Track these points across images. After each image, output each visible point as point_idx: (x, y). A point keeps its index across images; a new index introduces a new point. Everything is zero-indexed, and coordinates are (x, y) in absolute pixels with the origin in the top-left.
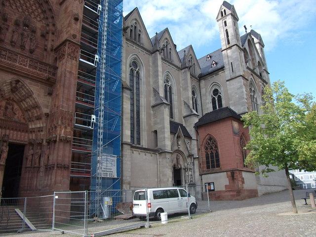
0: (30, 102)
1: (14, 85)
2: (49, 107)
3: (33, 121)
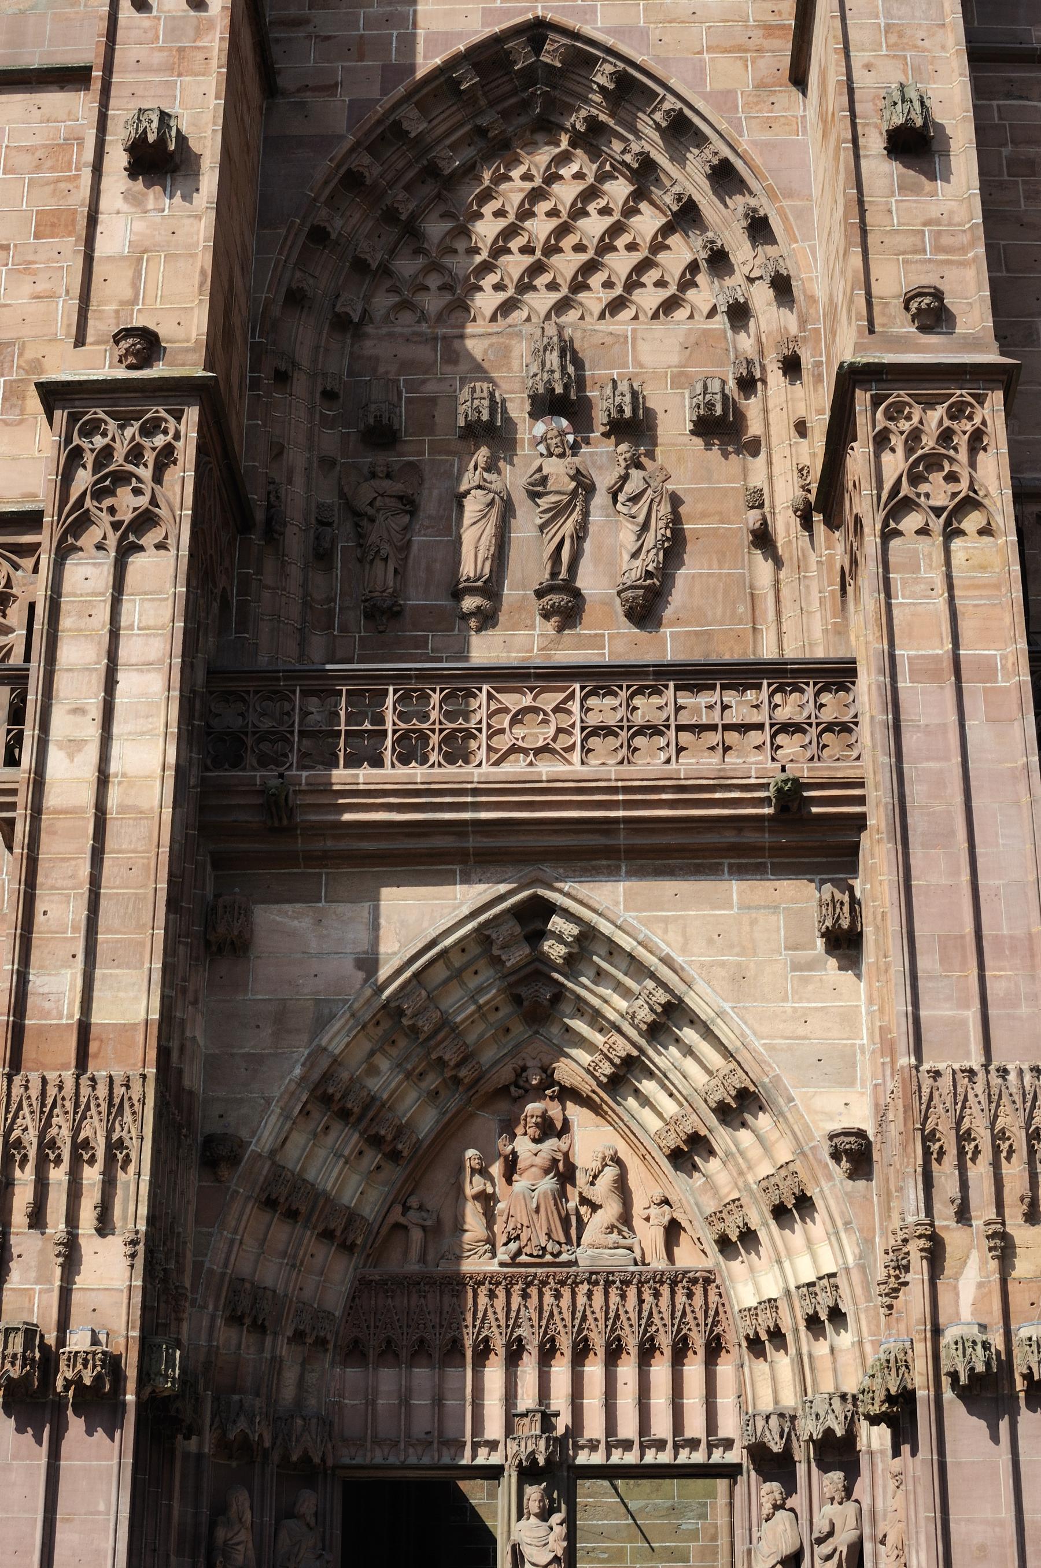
0: (689, 1073)
1: (517, 956)
2: (865, 1067)
3: (749, 1237)
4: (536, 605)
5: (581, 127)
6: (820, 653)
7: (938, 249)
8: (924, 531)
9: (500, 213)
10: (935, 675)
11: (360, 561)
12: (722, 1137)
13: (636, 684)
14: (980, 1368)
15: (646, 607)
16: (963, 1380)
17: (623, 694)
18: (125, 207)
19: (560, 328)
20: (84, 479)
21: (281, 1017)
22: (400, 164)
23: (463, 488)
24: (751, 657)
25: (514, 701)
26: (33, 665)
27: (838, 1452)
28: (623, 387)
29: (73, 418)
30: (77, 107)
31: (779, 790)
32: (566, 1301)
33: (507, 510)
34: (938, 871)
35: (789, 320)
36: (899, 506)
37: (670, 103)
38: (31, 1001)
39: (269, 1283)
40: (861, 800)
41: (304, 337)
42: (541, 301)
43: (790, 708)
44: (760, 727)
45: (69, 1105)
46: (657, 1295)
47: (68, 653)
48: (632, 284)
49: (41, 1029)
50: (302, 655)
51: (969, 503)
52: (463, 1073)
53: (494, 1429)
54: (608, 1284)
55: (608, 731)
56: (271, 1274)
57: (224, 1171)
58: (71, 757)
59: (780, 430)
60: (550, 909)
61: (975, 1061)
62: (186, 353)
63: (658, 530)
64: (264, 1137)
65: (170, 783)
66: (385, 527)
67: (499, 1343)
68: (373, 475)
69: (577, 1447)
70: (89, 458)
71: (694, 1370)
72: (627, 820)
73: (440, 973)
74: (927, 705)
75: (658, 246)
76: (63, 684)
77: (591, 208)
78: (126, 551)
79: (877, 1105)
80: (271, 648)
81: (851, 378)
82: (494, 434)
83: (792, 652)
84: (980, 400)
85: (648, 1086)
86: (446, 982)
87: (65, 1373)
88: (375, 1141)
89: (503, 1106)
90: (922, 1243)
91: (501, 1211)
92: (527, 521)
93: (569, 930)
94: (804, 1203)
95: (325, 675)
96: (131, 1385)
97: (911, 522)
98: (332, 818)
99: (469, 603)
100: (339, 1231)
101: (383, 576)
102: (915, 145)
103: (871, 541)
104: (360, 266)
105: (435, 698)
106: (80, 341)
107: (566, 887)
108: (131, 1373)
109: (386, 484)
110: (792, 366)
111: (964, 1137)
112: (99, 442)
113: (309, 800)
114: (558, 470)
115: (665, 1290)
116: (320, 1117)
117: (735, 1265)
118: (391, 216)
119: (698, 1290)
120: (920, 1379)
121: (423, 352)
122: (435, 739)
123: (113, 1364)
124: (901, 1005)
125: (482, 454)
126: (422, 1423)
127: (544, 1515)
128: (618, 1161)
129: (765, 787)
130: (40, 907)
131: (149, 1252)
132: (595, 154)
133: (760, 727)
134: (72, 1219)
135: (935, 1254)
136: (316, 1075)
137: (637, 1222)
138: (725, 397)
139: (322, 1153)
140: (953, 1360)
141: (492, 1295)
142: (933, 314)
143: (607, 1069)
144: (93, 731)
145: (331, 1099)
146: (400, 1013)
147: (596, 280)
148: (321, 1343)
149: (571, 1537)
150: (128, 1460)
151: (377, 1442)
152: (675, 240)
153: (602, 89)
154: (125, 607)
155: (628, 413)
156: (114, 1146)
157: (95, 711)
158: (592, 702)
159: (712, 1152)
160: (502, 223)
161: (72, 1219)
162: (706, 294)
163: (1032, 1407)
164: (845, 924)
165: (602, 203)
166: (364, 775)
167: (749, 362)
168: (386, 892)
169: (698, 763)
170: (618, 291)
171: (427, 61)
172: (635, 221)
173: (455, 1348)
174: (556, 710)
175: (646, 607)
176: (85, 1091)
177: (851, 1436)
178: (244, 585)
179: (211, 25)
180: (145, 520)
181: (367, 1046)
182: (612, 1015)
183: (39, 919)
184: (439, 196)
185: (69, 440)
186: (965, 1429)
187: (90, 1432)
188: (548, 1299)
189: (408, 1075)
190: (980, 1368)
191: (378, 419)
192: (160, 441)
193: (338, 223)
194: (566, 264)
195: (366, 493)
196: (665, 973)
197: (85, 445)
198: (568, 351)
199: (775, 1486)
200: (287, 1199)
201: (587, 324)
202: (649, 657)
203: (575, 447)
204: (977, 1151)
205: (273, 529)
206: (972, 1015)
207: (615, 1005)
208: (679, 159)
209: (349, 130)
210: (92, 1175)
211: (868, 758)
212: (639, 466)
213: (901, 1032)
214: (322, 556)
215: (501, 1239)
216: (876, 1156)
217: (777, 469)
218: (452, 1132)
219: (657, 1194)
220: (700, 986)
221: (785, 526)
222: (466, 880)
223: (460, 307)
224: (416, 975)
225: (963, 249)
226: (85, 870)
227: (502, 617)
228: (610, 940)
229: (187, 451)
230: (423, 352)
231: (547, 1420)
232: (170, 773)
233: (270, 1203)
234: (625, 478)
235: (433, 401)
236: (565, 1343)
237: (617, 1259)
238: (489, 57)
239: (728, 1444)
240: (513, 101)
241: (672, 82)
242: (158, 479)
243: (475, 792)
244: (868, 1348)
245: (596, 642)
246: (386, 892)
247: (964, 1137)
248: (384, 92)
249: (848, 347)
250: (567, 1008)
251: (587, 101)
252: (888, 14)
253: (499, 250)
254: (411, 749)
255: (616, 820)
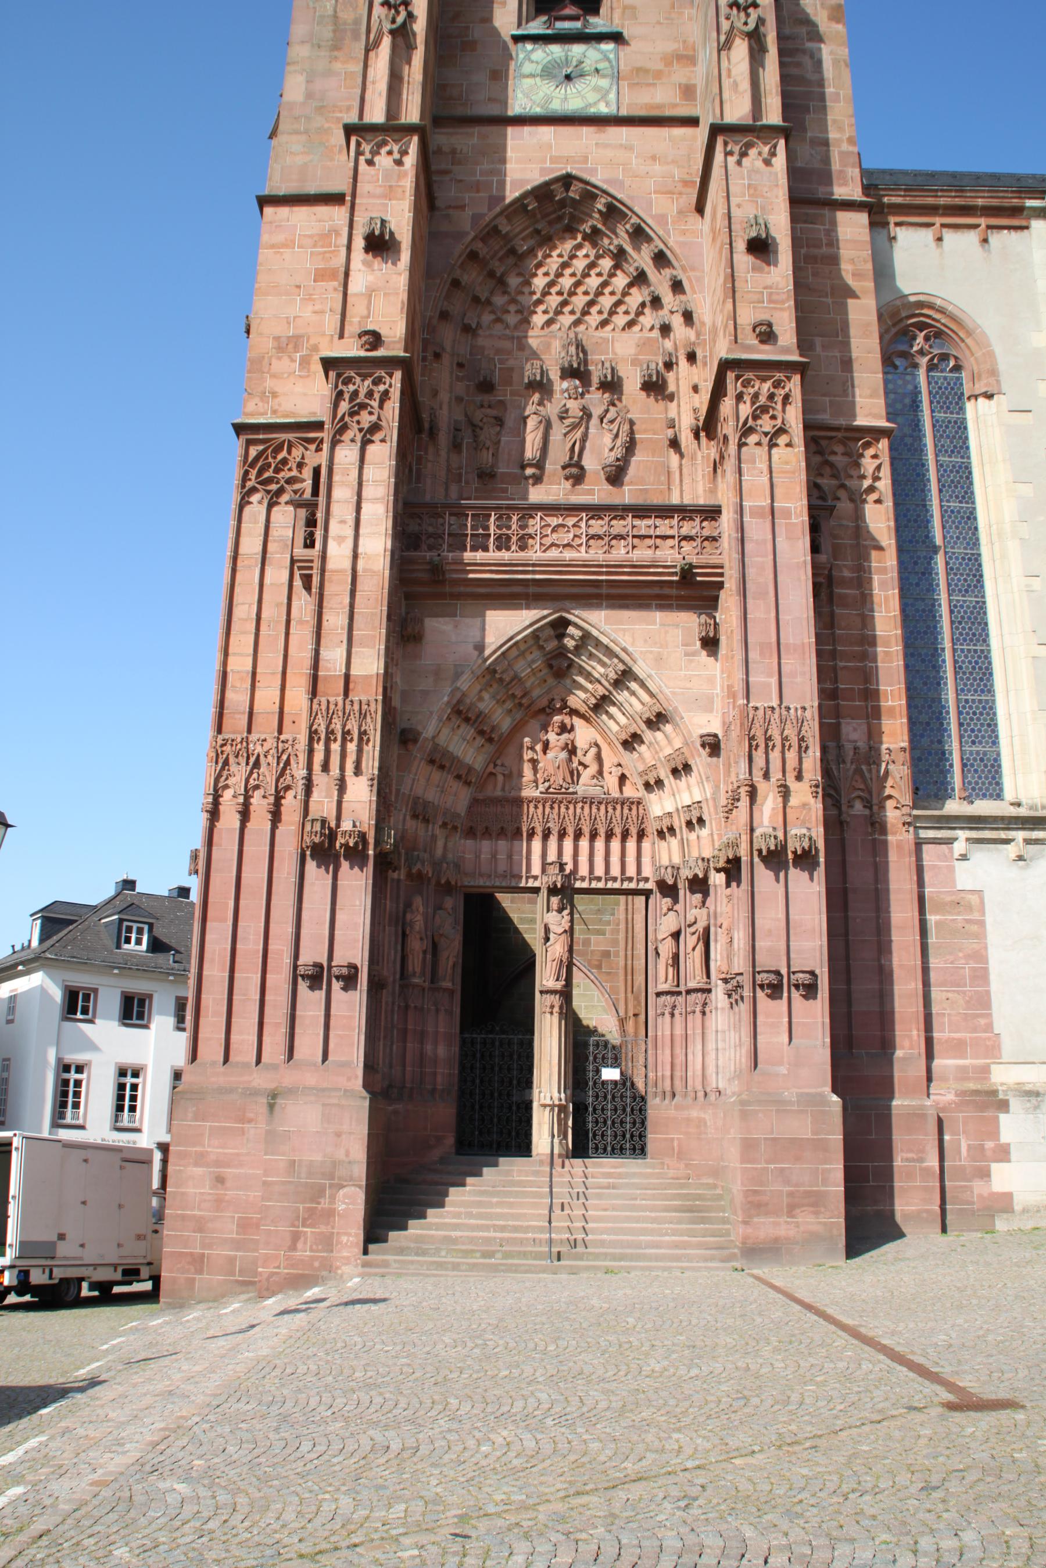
0: (633, 704)
1: (551, 645)
2: (718, 704)
4: (562, 473)
5: (588, 231)
6: (701, 502)
7: (770, 301)
8: (758, 444)
9: (546, 274)
10: (762, 516)
11: (475, 449)
12: (648, 735)
13: (613, 514)
14: (773, 848)
15: (616, 476)
16: (764, 853)
17: (607, 519)
18: (363, 268)
19: (576, 334)
20: (344, 406)
21: (437, 673)
22: (497, 248)
23: (527, 413)
24: (667, 503)
25: (554, 521)
26: (320, 499)
27: (700, 885)
28: (607, 365)
29: (339, 376)
30: (338, 215)
31: (682, 569)
32: (571, 811)
33: (548, 426)
34: (760, 611)
35: (691, 334)
36: (747, 431)
37: (635, 220)
38: (321, 663)
39: (430, 799)
40: (721, 575)
41: (448, 335)
42: (566, 320)
43: (687, 528)
44: (673, 537)
45: (340, 714)
46: (614, 809)
47: (338, 493)
48: (612, 313)
49: (326, 677)
50: (447, 495)
51: (781, 431)
52: (524, 701)
53: (536, 870)
54: (592, 803)
55: (599, 537)
56: (431, 795)
57: (410, 746)
58: (339, 544)
59: (685, 389)
60: (567, 623)
61: (775, 703)
62: (395, 345)
63: (623, 437)
64: (429, 731)
65: (388, 559)
66: (488, 433)
67: (539, 830)
68: (482, 406)
69: (575, 879)
70: (347, 396)
71: (631, 845)
72: (607, 581)
73: (515, 652)
74: (757, 530)
75: (625, 294)
76: (335, 508)
77: (593, 273)
78: (366, 443)
79: (724, 723)
80: (432, 492)
81: (725, 366)
82: (542, 387)
83: (686, 501)
84: (789, 379)
85: (612, 710)
86: (517, 657)
87: (340, 840)
88: (481, 733)
89: (542, 717)
90: (747, 788)
91: (541, 767)
92: (558, 431)
93: (577, 633)
94: (687, 768)
95: (461, 506)
96: (371, 846)
97: (752, 439)
98: (463, 576)
99: (529, 471)
100: (464, 776)
101: (486, 457)
102: (761, 247)
103: (732, 448)
104: (476, 300)
105: (515, 518)
106: (341, 336)
107: (576, 612)
108: (371, 841)
109: (489, 411)
110: (691, 357)
111: (768, 739)
112: (352, 388)
113: (453, 567)
114: (574, 406)
115: (619, 807)
116: (456, 721)
117: (652, 796)
118: (491, 274)
119: (634, 807)
120: (743, 852)
121: (506, 344)
122: (514, 539)
123: (363, 836)
124: (740, 675)
125: (536, 397)
126: (502, 867)
127: (560, 911)
128: (597, 745)
129: (675, 567)
130: (325, 617)
131: (379, 784)
132: (594, 245)
133: (673, 537)
134: (342, 768)
135: (753, 794)
136: (455, 701)
137: (606, 774)
138: (658, 372)
139: (456, 738)
140: (760, 843)
141: (536, 807)
142: (767, 335)
143: (593, 701)
144: (350, 532)
145: (461, 713)
146: (495, 671)
147: (594, 310)
148: (455, 828)
149: (572, 921)
150: (370, 881)
151: (481, 875)
152: (634, 291)
153: (600, 211)
154: (365, 471)
155: (609, 378)
156: (362, 734)
157: (351, 523)
158: (592, 522)
159: (642, 742)
160: (547, 279)
161: (342, 768)
162: (649, 318)
163: (795, 867)
164: (711, 634)
165: (597, 270)
166: (479, 556)
167: (670, 355)
168: (489, 613)
169: (642, 554)
170: (605, 316)
171: (512, 194)
172: (614, 280)
173: (518, 832)
174: (574, 526)
175: (616, 476)
176: (348, 707)
177: (706, 878)
178: (419, 459)
179: (406, 174)
180: (375, 428)
181: (478, 687)
182: (597, 675)
183: (325, 624)
184: (515, 264)
185: (336, 387)
186: (764, 876)
187: (352, 868)
188: (563, 810)
189: (498, 702)
190: (773, 848)
191: (485, 378)
192: (382, 388)
193: (466, 277)
194: (579, 301)
195: (478, 415)
196: (623, 655)
197: (344, 388)
198: (580, 347)
199: (669, 900)
200: (439, 760)
201: (589, 332)
202: (616, 501)
203: (582, 395)
204: (774, 746)
205: (433, 433)
206: (774, 681)
207: (598, 671)
208: (637, 249)
209: (472, 228)
210: (352, 747)
211: (726, 554)
212: (614, 405)
213: (739, 687)
214: (456, 446)
215: (541, 781)
216: (722, 746)
217: (682, 409)
218: (517, 729)
219: (616, 761)
220: (640, 662)
221: (686, 438)
222: (528, 608)
223: (526, 322)
224: (503, 654)
225: (783, 302)
226: (347, 600)
227: (545, 479)
228: (597, 639)
229: (396, 394)
230: (506, 344)
231: (562, 866)
232: (388, 553)
233: (432, 762)
234: (607, 411)
235: (511, 369)
236: (570, 831)
237: (595, 791)
238: (542, 193)
239: (646, 880)
240: (553, 216)
241: (636, 209)
242: (381, 407)
243: (534, 565)
244: (716, 837)
245: (591, 492)
246: (489, 613)
247: (768, 739)
248: (490, 210)
249: (723, 350)
250: (574, 671)
251: (591, 217)
252: (749, 178)
253: (546, 293)
254: (503, 543)
255: (602, 581)
